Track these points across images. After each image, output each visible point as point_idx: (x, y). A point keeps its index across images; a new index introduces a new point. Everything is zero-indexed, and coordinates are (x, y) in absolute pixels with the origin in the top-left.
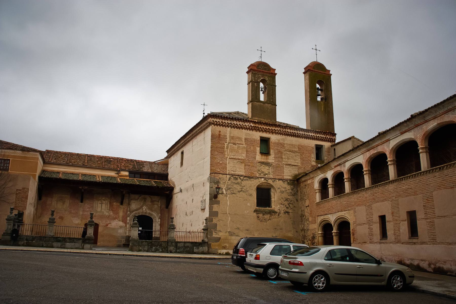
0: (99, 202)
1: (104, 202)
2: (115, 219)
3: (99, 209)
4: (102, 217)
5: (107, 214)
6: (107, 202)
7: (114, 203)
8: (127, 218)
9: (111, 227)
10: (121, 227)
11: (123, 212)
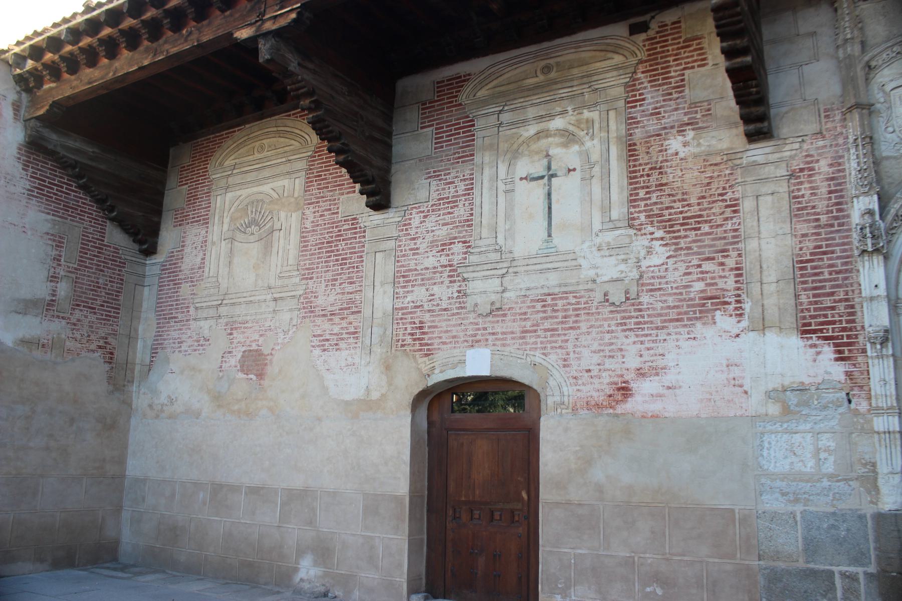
0: (524, 167)
1: (566, 156)
2: (713, 302)
3: (527, 238)
4: (559, 311)
5: (610, 268)
6: (594, 146)
7: (675, 144)
8: (846, 274)
9: (669, 408)
10: (793, 400)
11: (798, 209)
